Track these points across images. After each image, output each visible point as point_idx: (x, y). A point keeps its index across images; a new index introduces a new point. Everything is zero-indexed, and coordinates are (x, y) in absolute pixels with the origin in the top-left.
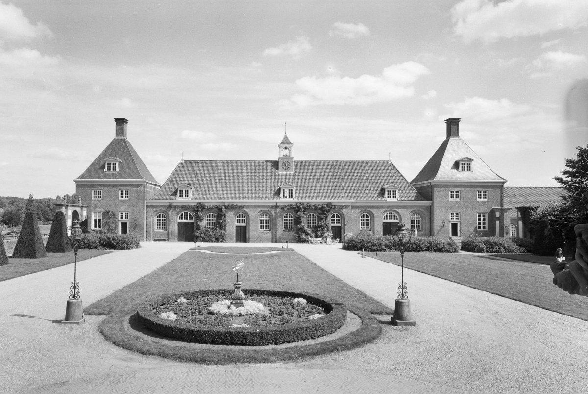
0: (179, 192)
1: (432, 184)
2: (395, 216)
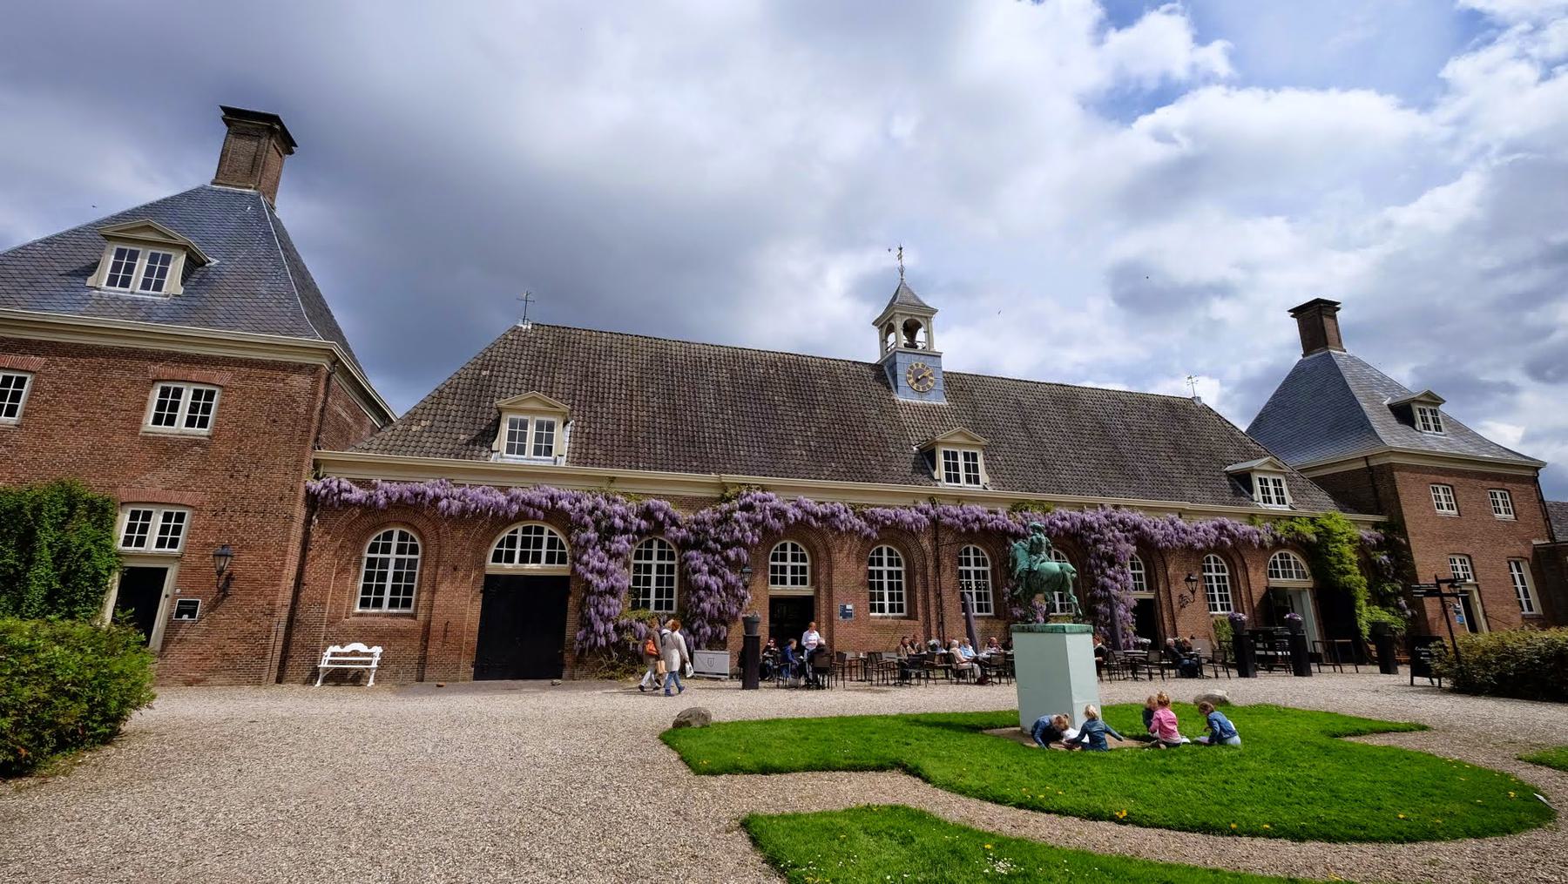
0: (505, 428)
1: (1373, 463)
2: (1296, 563)
